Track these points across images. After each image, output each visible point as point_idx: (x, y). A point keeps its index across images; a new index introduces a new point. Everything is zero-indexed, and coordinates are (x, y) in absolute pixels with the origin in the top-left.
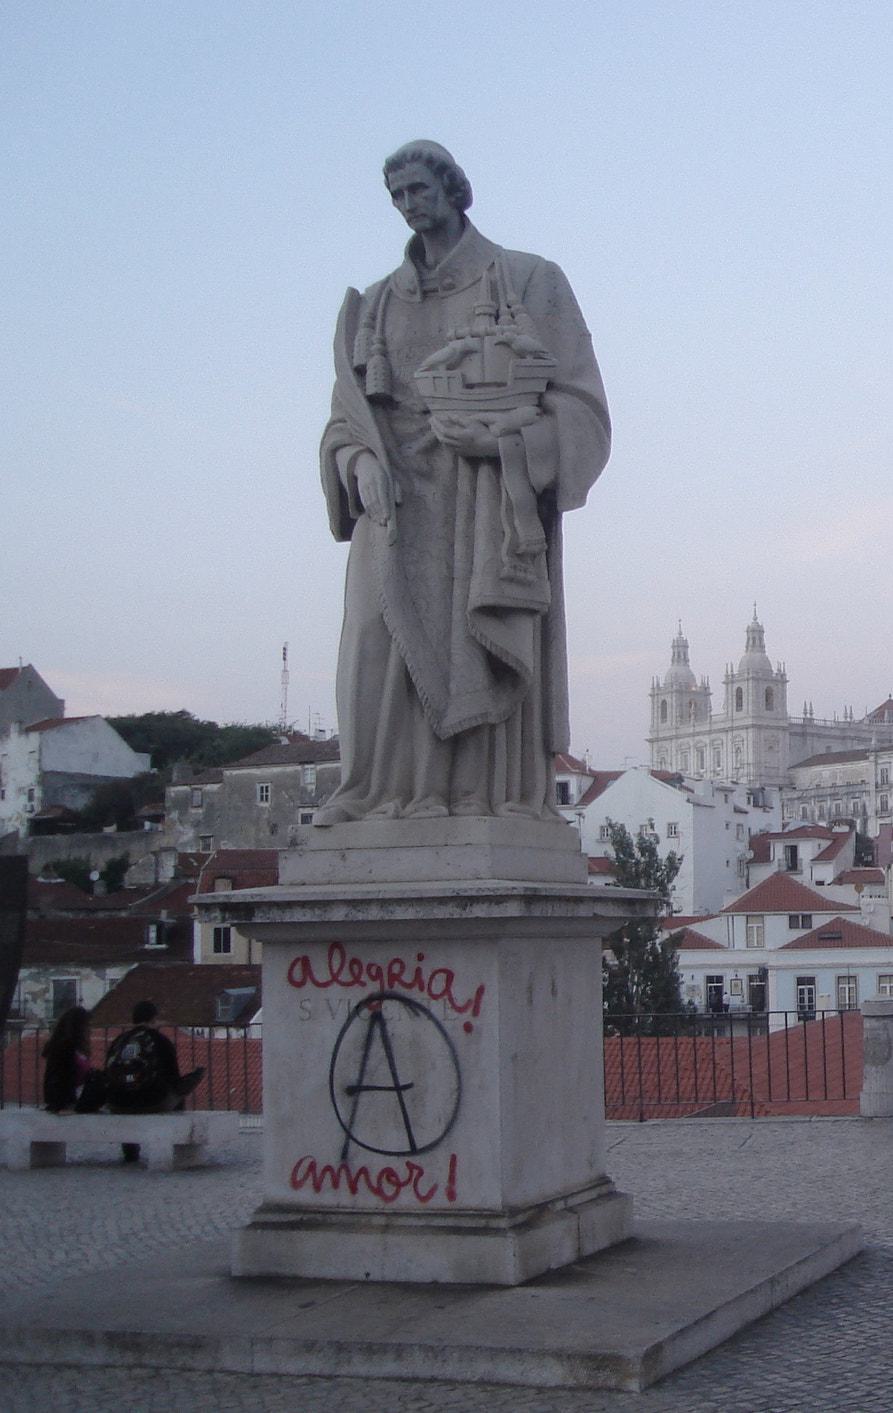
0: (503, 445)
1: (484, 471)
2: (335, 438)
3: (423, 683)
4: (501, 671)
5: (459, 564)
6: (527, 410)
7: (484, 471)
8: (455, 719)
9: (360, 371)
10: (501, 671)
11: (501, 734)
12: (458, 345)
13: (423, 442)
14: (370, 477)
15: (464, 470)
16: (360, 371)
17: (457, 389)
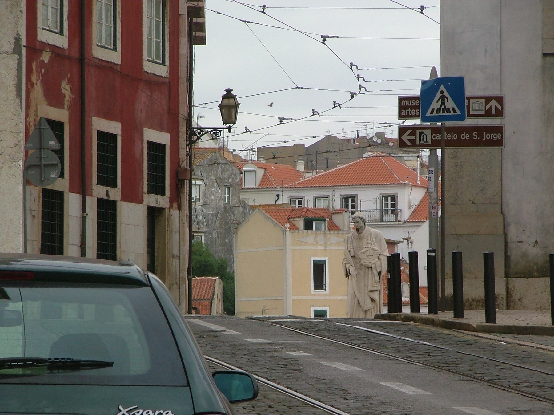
0: (373, 266)
1: (370, 269)
2: (345, 262)
3: (361, 303)
4: (373, 300)
5: (366, 284)
6: (377, 260)
7: (370, 269)
8: (366, 308)
9: (349, 251)
10: (373, 300)
11: (373, 310)
12: (366, 249)
13: (360, 263)
14: (352, 270)
15: (367, 269)
16: (349, 251)
17: (365, 257)
